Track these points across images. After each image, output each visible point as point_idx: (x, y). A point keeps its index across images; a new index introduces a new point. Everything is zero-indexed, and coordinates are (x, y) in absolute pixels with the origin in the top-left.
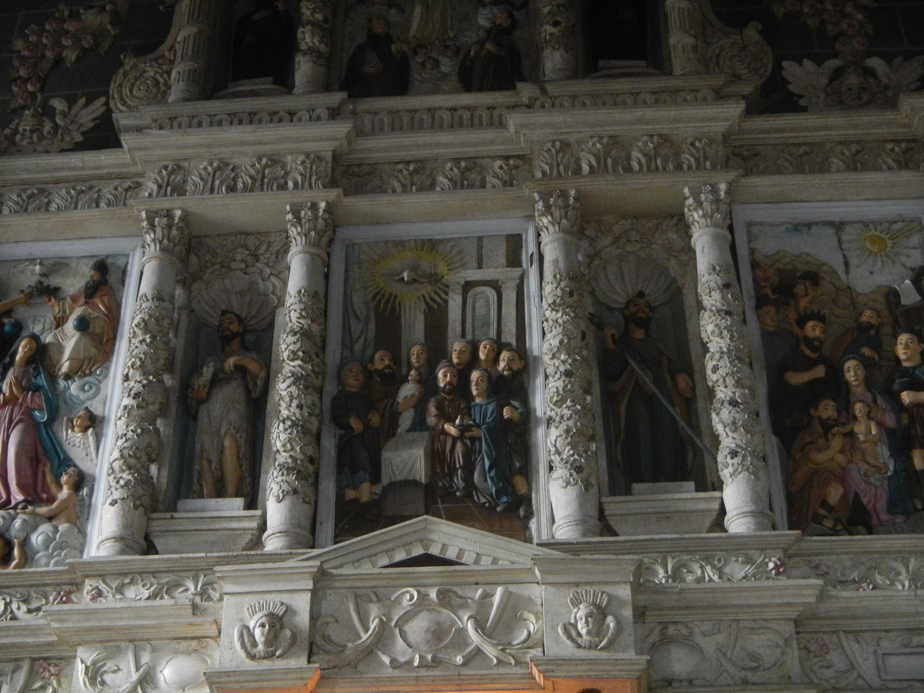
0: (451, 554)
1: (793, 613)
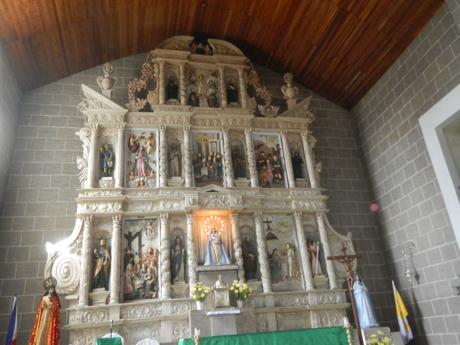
0: (216, 190)
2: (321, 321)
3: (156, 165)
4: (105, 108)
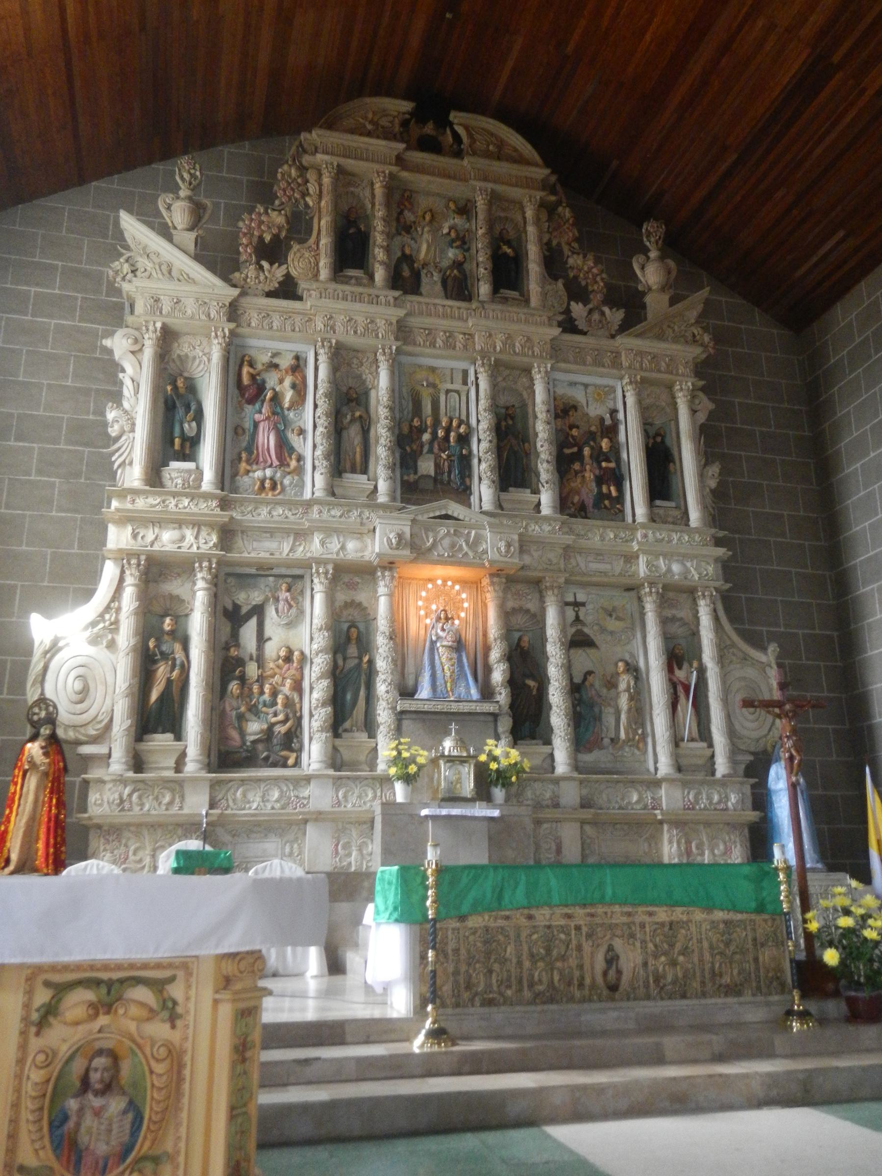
0: (455, 515)
1: (563, 546)
2: (686, 849)
3: (305, 439)
4: (179, 280)
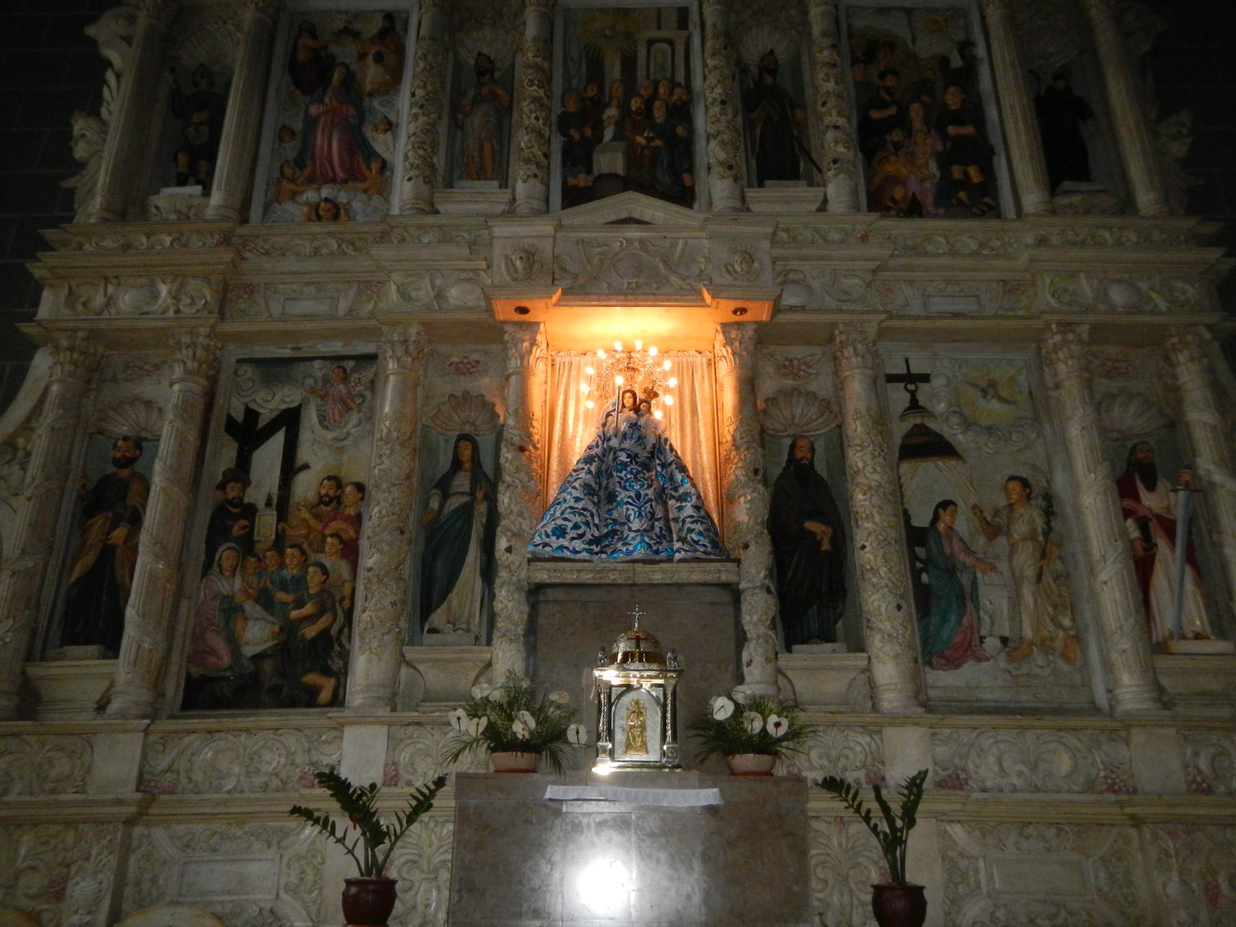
0: (647, 218)
1: (872, 265)
